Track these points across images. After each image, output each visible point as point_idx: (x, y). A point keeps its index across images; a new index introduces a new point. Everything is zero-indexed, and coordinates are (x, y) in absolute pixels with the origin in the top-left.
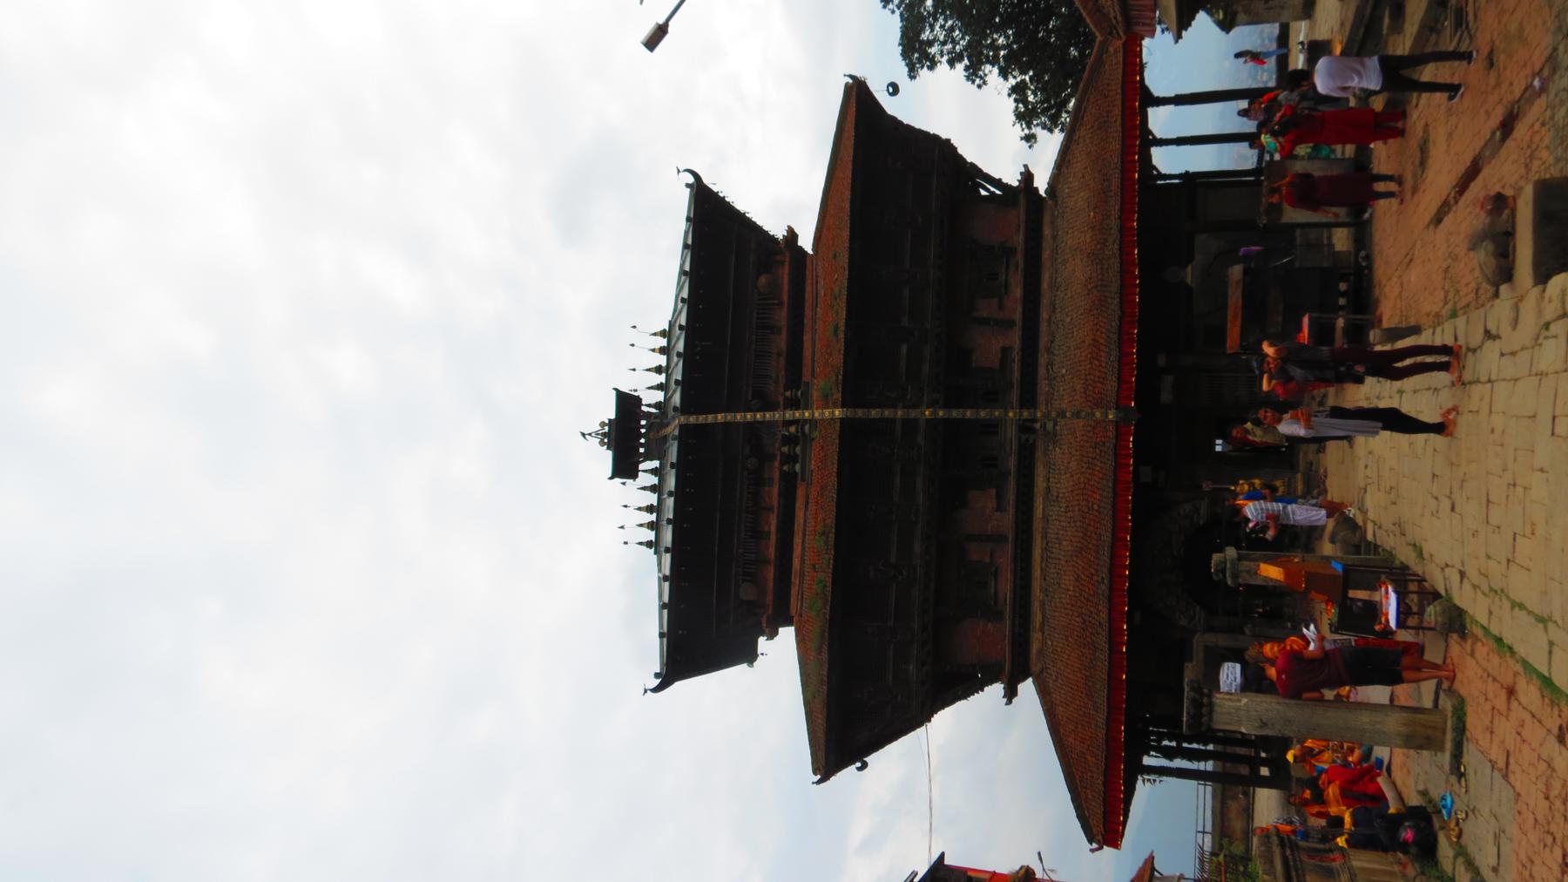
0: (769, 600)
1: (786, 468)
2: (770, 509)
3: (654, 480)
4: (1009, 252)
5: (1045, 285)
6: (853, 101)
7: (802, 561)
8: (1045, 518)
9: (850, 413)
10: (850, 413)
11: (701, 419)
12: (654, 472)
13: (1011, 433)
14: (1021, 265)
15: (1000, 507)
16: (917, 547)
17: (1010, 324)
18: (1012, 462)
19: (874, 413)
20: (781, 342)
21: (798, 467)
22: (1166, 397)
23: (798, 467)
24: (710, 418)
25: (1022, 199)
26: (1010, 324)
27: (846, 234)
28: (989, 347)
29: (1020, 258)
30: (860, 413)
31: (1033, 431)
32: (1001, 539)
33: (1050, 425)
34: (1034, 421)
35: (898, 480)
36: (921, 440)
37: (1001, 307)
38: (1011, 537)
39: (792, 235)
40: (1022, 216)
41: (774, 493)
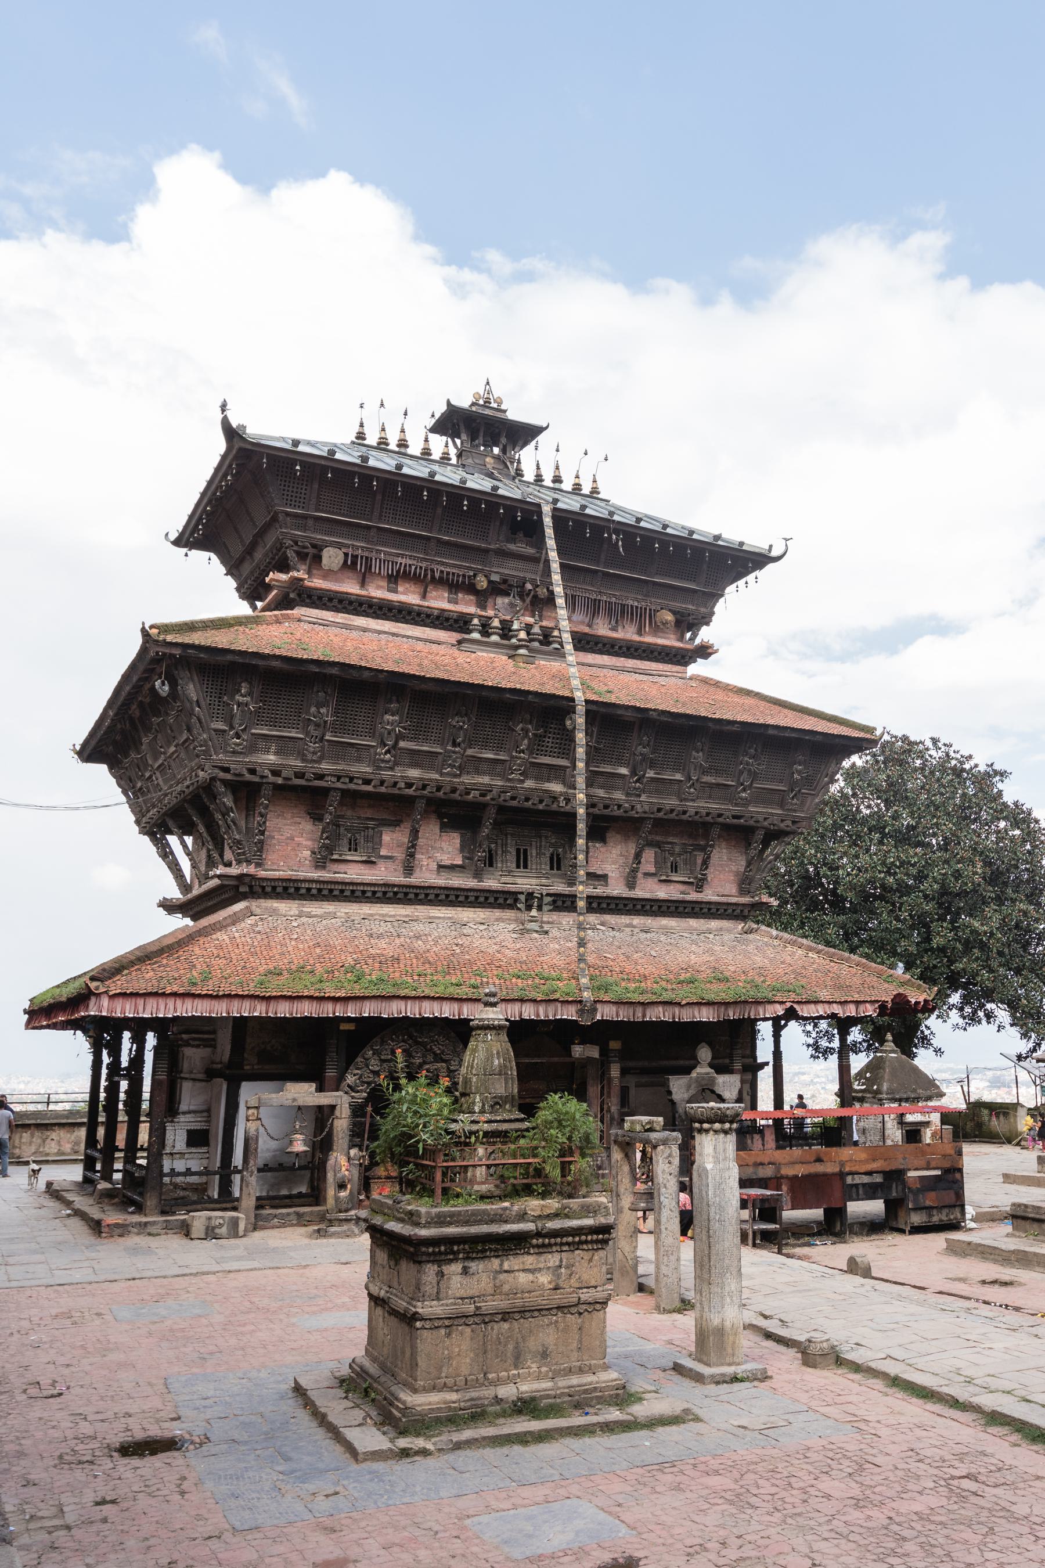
0: (318, 583)
1: (476, 621)
2: (424, 597)
3: (436, 455)
4: (699, 885)
5: (665, 921)
6: (862, 735)
7: (365, 630)
8: (431, 920)
9: (581, 709)
10: (581, 709)
11: (549, 532)
12: (445, 458)
13: (524, 882)
14: (688, 898)
15: (441, 867)
16: (414, 773)
17: (631, 885)
18: (491, 883)
19: (580, 737)
20: (602, 629)
21: (476, 635)
22: (577, 1051)
23: (476, 635)
24: (551, 543)
25: (746, 900)
26: (631, 885)
27: (750, 719)
28: (610, 863)
29: (693, 896)
30: (581, 720)
31: (529, 908)
32: (409, 870)
33: (534, 926)
34: (540, 908)
35: (490, 756)
36: (529, 784)
37: (647, 875)
38: (413, 880)
39: (705, 651)
40: (734, 900)
41: (439, 601)
